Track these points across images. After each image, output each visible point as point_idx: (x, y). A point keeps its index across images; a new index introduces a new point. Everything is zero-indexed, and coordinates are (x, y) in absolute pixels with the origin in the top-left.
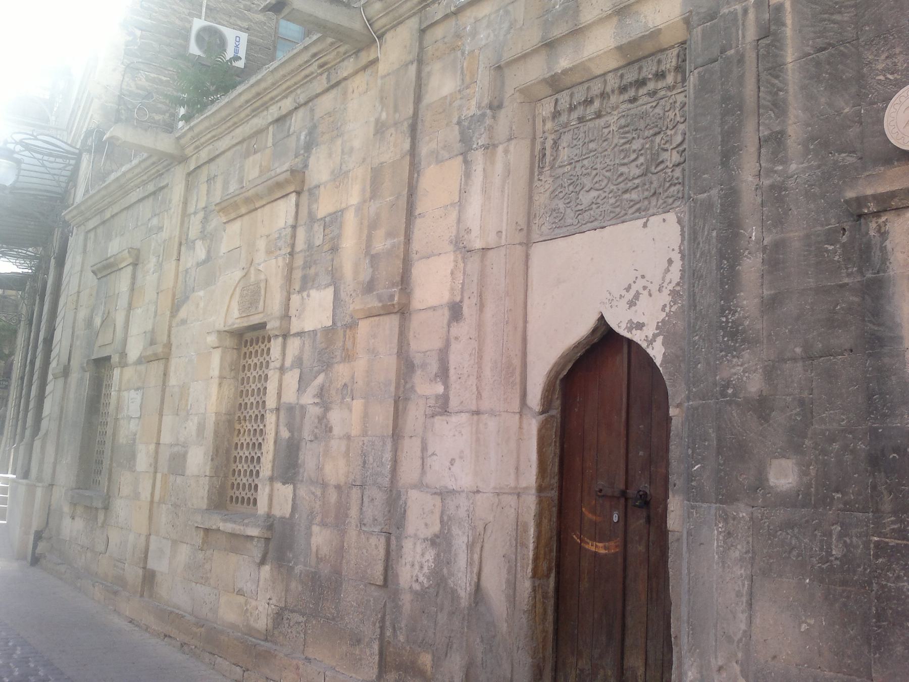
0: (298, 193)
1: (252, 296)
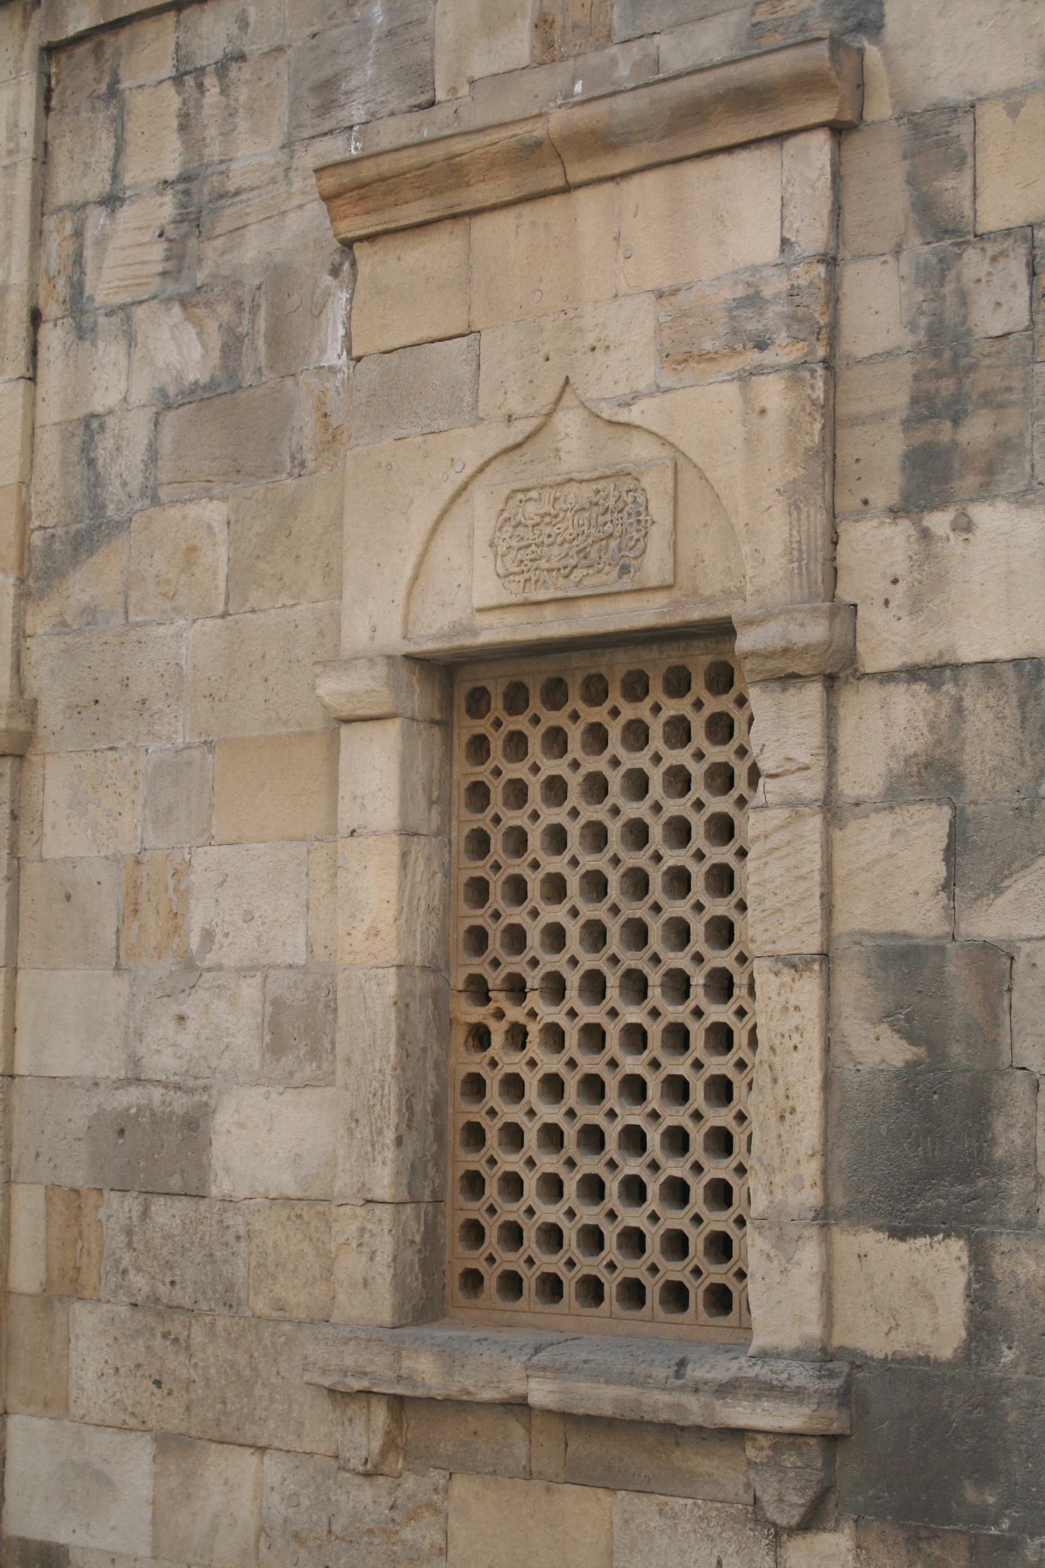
0: (839, 130)
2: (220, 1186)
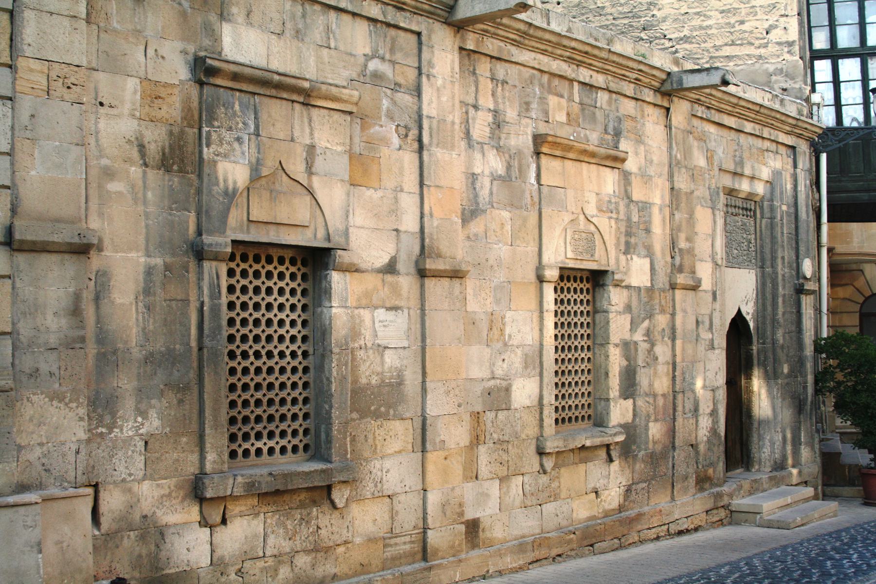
1: (588, 241)
2: (515, 405)
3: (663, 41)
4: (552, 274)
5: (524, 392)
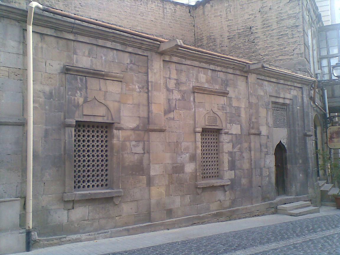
3: (260, 56)
4: (199, 129)
5: (190, 168)
